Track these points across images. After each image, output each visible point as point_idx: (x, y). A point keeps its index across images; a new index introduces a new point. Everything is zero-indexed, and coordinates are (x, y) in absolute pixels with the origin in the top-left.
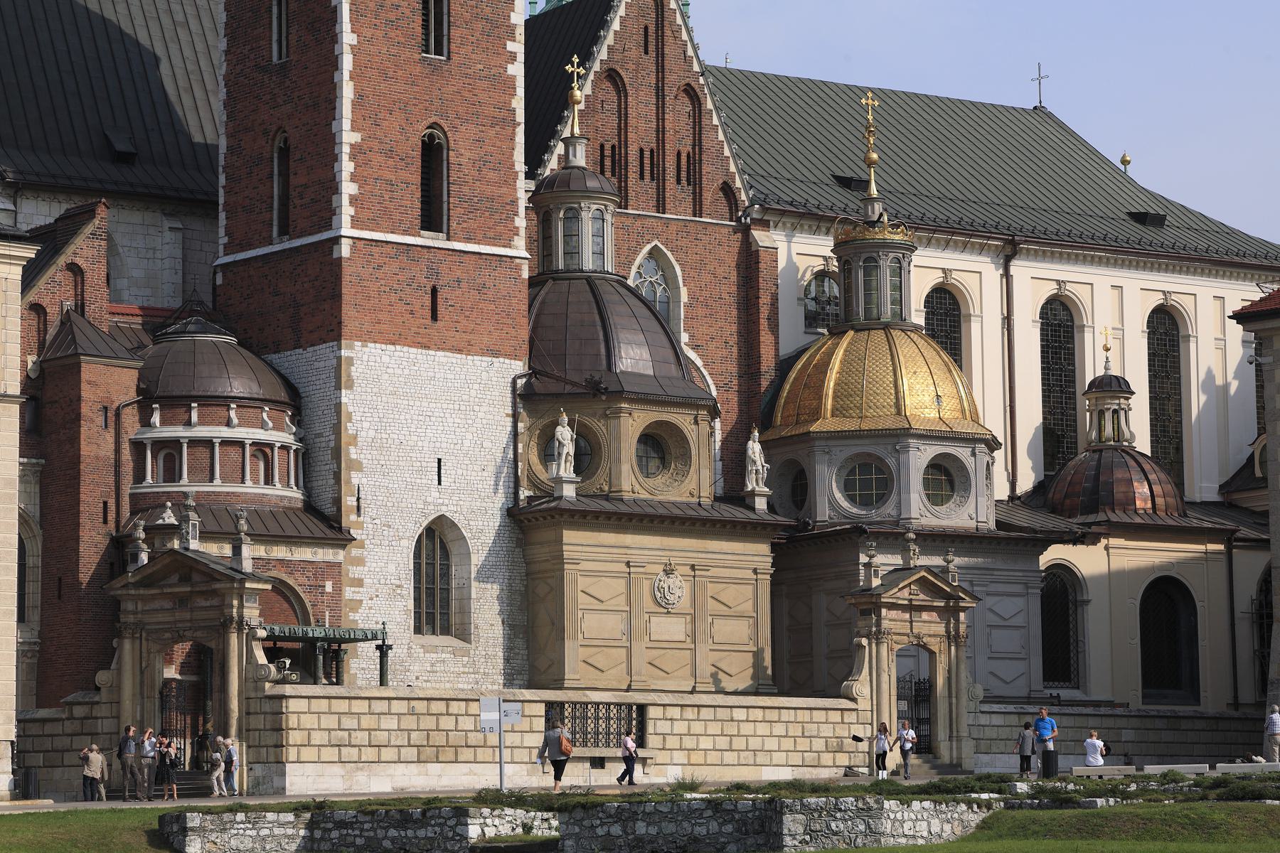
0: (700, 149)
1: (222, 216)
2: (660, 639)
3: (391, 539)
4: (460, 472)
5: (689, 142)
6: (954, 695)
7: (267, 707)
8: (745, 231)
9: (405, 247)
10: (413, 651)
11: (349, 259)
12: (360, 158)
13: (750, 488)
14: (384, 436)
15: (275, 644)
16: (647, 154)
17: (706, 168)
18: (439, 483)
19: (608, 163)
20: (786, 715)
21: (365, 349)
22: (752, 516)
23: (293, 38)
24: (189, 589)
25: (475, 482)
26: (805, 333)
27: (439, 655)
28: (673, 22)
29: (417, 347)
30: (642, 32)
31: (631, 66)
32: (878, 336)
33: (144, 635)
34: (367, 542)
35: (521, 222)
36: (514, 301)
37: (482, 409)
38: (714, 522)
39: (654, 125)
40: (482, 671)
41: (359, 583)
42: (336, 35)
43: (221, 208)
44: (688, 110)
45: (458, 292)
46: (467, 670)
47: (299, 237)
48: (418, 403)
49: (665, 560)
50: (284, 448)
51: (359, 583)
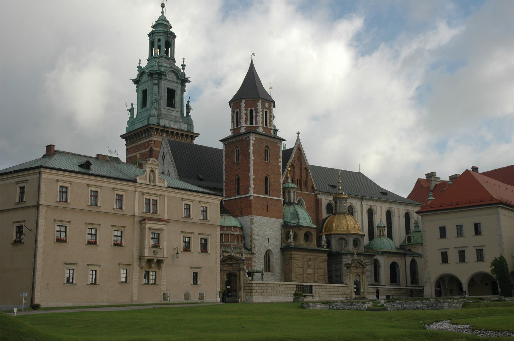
0: (308, 179)
1: (224, 191)
5: (306, 178)
6: (364, 283)
7: (250, 285)
8: (316, 195)
11: (253, 200)
13: (323, 244)
16: (298, 180)
17: (309, 183)
20: (336, 288)
21: (256, 217)
22: (323, 249)
24: (232, 263)
26: (327, 215)
28: (303, 156)
31: (296, 164)
32: (343, 215)
33: (222, 271)
34: (256, 254)
35: (282, 193)
39: (300, 175)
41: (255, 262)
42: (250, 157)
43: (224, 190)
47: (242, 195)
49: (309, 258)
50: (241, 236)
51: (255, 262)
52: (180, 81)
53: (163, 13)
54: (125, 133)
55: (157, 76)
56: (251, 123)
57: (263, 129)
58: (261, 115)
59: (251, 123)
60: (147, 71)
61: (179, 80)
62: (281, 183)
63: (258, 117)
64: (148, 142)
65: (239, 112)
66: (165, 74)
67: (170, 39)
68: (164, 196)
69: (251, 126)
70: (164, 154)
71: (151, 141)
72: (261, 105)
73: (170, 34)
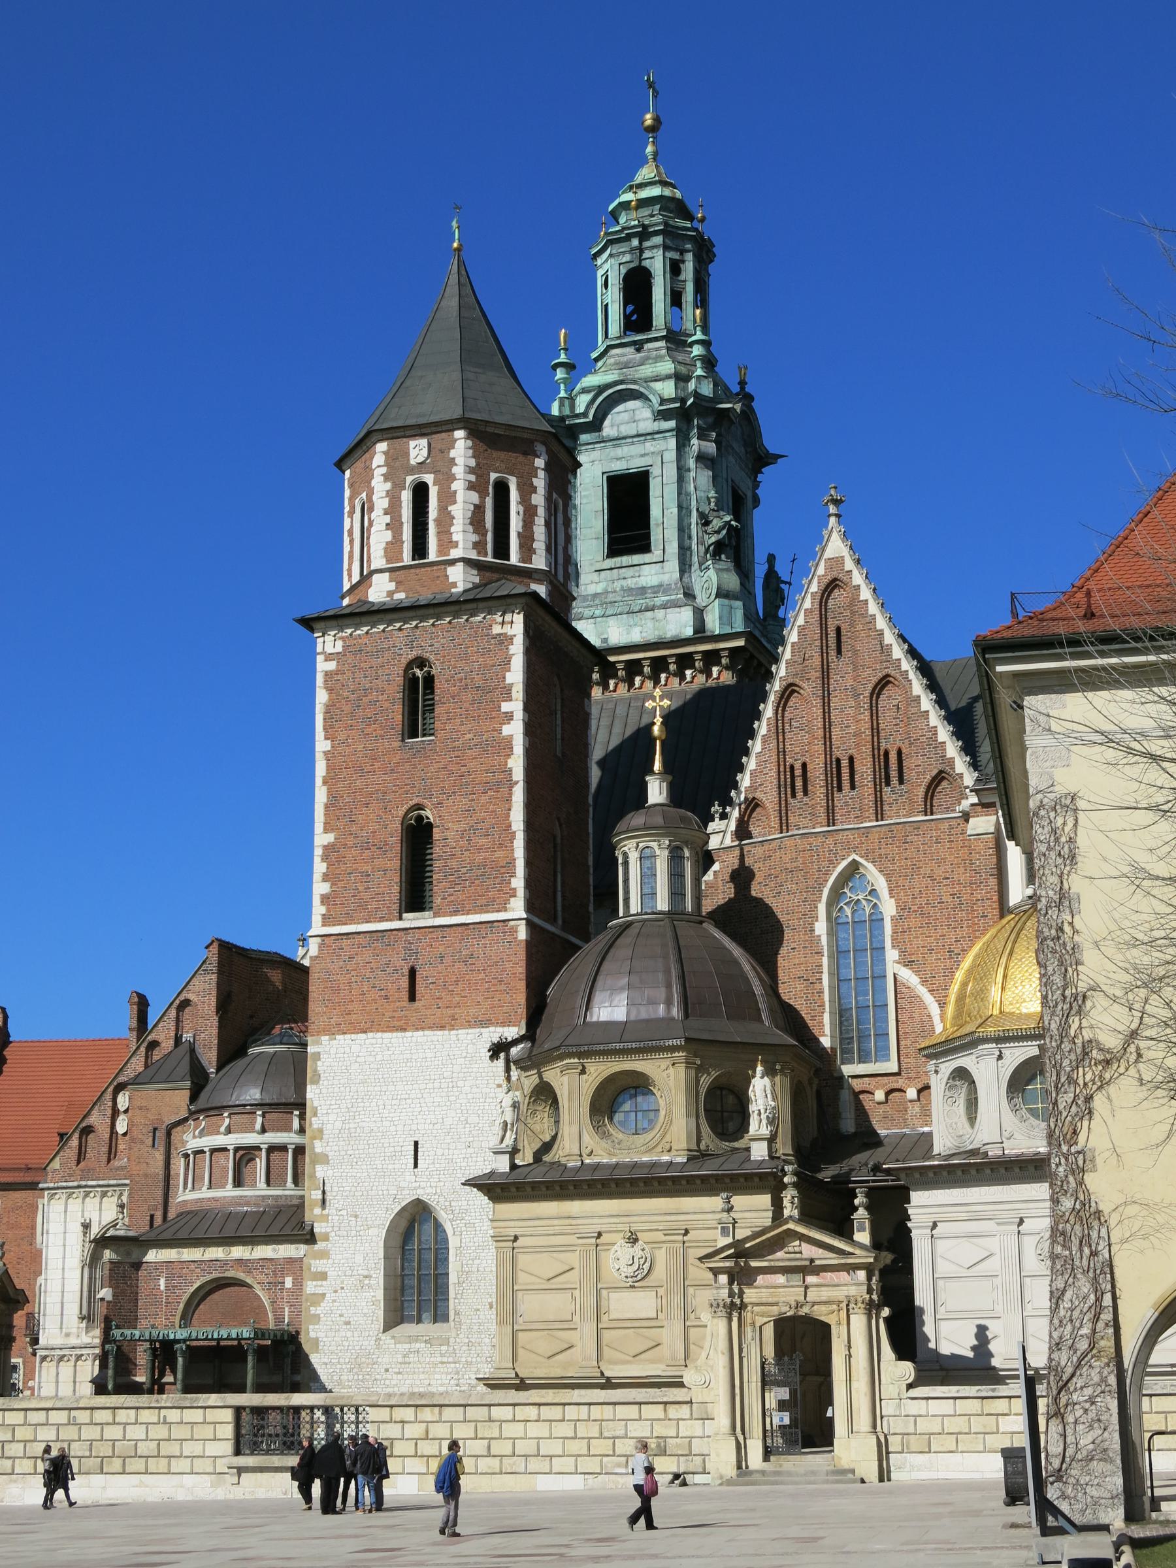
2: (621, 1317)
3: (358, 1228)
4: (439, 1152)
8: (966, 817)
9: (380, 934)
10: (381, 1342)
11: (317, 957)
12: (333, 858)
14: (352, 1125)
15: (218, 1343)
16: (845, 763)
18: (416, 1166)
19: (799, 783)
20: (571, 1412)
25: (458, 1160)
27: (413, 1345)
29: (390, 1031)
30: (832, 635)
31: (815, 674)
34: (333, 1234)
35: (518, 882)
36: (509, 965)
37: (468, 1083)
38: (690, 1179)
40: (464, 1359)
41: (323, 1276)
44: (895, 702)
45: (441, 968)
46: (445, 1360)
48: (391, 1088)
49: (621, 1227)
51: (323, 1276)
57: (390, 581)
58: (386, 513)
61: (666, 419)
62: (514, 828)
63: (373, 530)
66: (582, 420)
72: (387, 464)
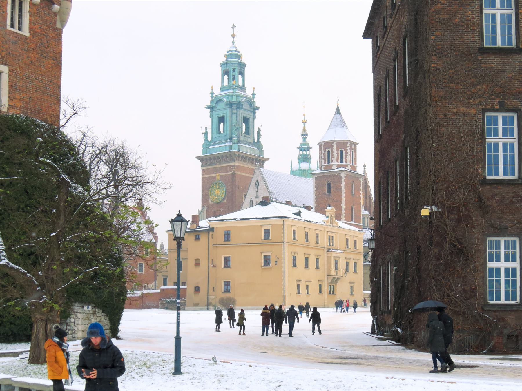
23: (332, 190)
35: (361, 220)
52: (252, 110)
53: (233, 43)
54: (200, 154)
55: (236, 105)
56: (342, 162)
59: (342, 162)
60: (225, 100)
64: (230, 166)
65: (330, 152)
67: (243, 69)
68: (337, 233)
69: (341, 165)
70: (257, 181)
71: (234, 165)
73: (243, 65)
